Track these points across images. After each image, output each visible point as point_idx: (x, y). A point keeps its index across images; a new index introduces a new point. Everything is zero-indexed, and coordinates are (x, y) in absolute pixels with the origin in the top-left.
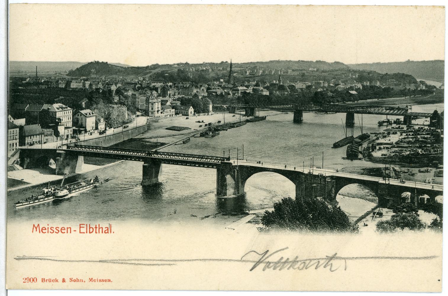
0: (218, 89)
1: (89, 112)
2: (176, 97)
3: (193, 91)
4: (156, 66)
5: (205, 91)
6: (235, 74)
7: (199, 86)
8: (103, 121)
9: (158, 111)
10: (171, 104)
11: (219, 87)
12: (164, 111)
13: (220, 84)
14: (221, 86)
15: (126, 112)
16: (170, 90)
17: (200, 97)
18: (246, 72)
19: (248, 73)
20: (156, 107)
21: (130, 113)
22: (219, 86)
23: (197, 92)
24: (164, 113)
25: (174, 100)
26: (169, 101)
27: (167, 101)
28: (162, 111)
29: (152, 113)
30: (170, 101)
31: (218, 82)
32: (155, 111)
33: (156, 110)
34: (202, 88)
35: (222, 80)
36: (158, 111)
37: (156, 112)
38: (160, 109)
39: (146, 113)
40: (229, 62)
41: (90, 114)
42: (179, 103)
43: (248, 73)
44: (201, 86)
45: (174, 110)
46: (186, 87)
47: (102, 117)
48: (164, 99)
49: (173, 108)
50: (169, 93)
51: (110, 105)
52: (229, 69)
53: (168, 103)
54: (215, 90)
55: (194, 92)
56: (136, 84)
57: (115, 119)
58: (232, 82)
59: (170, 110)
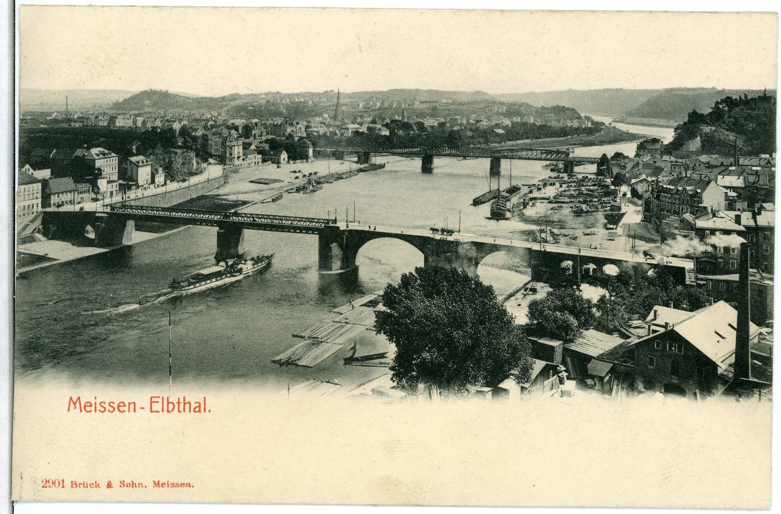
0: (321, 127)
1: (142, 159)
2: (264, 138)
3: (286, 130)
4: (234, 97)
5: (303, 130)
6: (344, 108)
7: (294, 123)
8: (161, 172)
9: (238, 158)
10: (256, 148)
11: (323, 125)
12: (246, 157)
13: (324, 121)
14: (324, 123)
15: (195, 158)
16: (255, 128)
17: (296, 139)
18: (358, 105)
19: (361, 107)
20: (236, 152)
21: (200, 161)
22: (322, 123)
23: (292, 131)
24: (247, 161)
25: (260, 142)
26: (253, 143)
27: (250, 144)
28: (244, 157)
29: (231, 159)
30: (256, 144)
31: (321, 119)
32: (234, 158)
33: (236, 156)
34: (299, 126)
35: (326, 116)
36: (238, 158)
37: (236, 159)
38: (241, 155)
39: (222, 160)
40: (336, 91)
41: (143, 162)
42: (267, 147)
43: (361, 107)
44: (298, 123)
45: (260, 156)
46: (277, 125)
47: (161, 166)
48: (247, 141)
49: (258, 154)
50: (253, 132)
51: (172, 150)
52: (335, 101)
53: (253, 147)
54: (316, 129)
55: (288, 131)
56: (209, 121)
57: (178, 169)
58: (340, 118)
59: (255, 156)
